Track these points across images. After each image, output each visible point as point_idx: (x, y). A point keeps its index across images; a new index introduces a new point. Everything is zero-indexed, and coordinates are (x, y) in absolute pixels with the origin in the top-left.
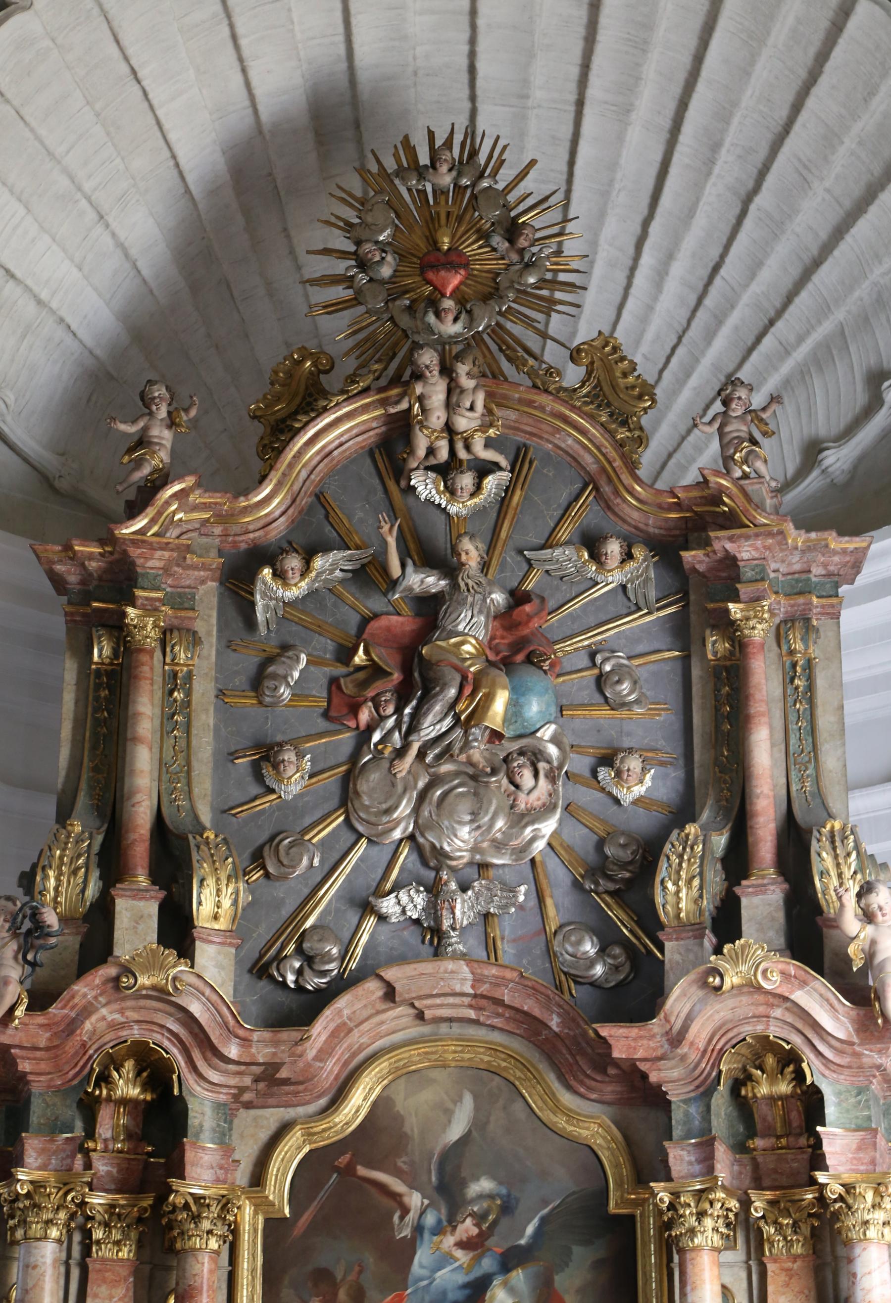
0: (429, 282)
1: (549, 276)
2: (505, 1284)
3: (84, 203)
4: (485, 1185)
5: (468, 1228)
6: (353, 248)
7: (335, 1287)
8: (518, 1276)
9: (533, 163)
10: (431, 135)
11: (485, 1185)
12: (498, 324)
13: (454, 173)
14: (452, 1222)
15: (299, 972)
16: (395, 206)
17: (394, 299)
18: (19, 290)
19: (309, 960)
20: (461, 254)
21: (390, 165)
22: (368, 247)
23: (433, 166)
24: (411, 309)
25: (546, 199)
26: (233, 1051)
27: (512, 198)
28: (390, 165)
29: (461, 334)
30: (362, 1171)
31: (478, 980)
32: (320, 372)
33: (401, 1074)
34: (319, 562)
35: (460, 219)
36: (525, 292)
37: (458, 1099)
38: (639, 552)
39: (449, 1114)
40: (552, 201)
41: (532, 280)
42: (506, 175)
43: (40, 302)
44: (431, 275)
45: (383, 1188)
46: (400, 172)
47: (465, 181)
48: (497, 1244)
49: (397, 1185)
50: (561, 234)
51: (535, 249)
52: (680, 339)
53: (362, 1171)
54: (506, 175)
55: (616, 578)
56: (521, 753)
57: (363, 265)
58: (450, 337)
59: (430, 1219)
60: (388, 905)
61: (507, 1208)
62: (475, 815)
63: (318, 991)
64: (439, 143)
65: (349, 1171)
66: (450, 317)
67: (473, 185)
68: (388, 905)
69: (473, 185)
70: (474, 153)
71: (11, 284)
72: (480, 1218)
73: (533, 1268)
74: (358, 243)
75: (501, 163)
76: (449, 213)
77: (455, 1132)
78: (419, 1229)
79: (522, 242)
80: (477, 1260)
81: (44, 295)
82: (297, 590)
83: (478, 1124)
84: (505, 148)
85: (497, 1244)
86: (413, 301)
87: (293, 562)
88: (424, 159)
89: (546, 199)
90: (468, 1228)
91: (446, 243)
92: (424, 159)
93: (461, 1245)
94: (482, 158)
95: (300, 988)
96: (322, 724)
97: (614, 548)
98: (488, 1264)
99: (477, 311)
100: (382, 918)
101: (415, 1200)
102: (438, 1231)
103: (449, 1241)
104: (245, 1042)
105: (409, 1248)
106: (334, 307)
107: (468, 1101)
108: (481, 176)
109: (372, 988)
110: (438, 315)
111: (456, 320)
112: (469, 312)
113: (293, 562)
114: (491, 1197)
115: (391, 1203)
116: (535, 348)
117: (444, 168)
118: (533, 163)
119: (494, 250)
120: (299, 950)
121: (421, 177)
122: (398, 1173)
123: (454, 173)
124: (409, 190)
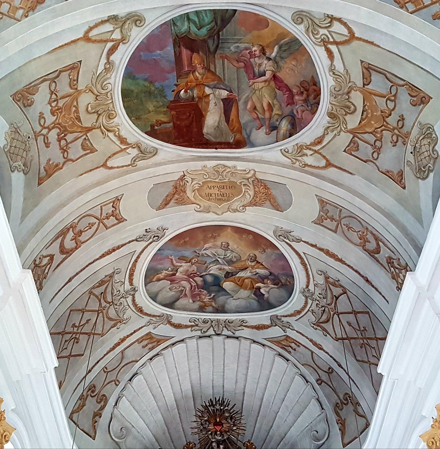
0: (215, 428)
1: (238, 427)
3: (149, 412)
6: (200, 421)
9: (235, 404)
10: (216, 398)
12: (229, 437)
13: (220, 406)
16: (208, 412)
17: (208, 432)
18: (135, 429)
20: (221, 423)
21: (208, 404)
22: (203, 421)
23: (216, 405)
24: (211, 434)
25: (238, 412)
27: (231, 411)
28: (208, 404)
29: (221, 439)
32: (193, 447)
35: (221, 415)
36: (234, 431)
40: (239, 412)
41: (235, 428)
42: (230, 407)
43: (138, 432)
44: (215, 427)
46: (210, 406)
47: (222, 408)
50: (241, 419)
51: (236, 422)
52: (264, 442)
54: (230, 407)
58: (219, 440)
64: (217, 400)
66: (219, 435)
67: (224, 408)
69: (224, 408)
70: (224, 402)
71: (133, 429)
74: (201, 420)
75: (229, 404)
76: (219, 414)
79: (233, 420)
81: (139, 431)
84: (230, 401)
86: (212, 432)
89: (238, 412)
91: (218, 420)
99: (224, 435)
106: (196, 433)
108: (225, 407)
110: (217, 435)
111: (220, 436)
112: (223, 435)
116: (236, 442)
117: (218, 405)
118: (235, 404)
119: (228, 422)
121: (214, 407)
123: (220, 406)
124: (211, 409)
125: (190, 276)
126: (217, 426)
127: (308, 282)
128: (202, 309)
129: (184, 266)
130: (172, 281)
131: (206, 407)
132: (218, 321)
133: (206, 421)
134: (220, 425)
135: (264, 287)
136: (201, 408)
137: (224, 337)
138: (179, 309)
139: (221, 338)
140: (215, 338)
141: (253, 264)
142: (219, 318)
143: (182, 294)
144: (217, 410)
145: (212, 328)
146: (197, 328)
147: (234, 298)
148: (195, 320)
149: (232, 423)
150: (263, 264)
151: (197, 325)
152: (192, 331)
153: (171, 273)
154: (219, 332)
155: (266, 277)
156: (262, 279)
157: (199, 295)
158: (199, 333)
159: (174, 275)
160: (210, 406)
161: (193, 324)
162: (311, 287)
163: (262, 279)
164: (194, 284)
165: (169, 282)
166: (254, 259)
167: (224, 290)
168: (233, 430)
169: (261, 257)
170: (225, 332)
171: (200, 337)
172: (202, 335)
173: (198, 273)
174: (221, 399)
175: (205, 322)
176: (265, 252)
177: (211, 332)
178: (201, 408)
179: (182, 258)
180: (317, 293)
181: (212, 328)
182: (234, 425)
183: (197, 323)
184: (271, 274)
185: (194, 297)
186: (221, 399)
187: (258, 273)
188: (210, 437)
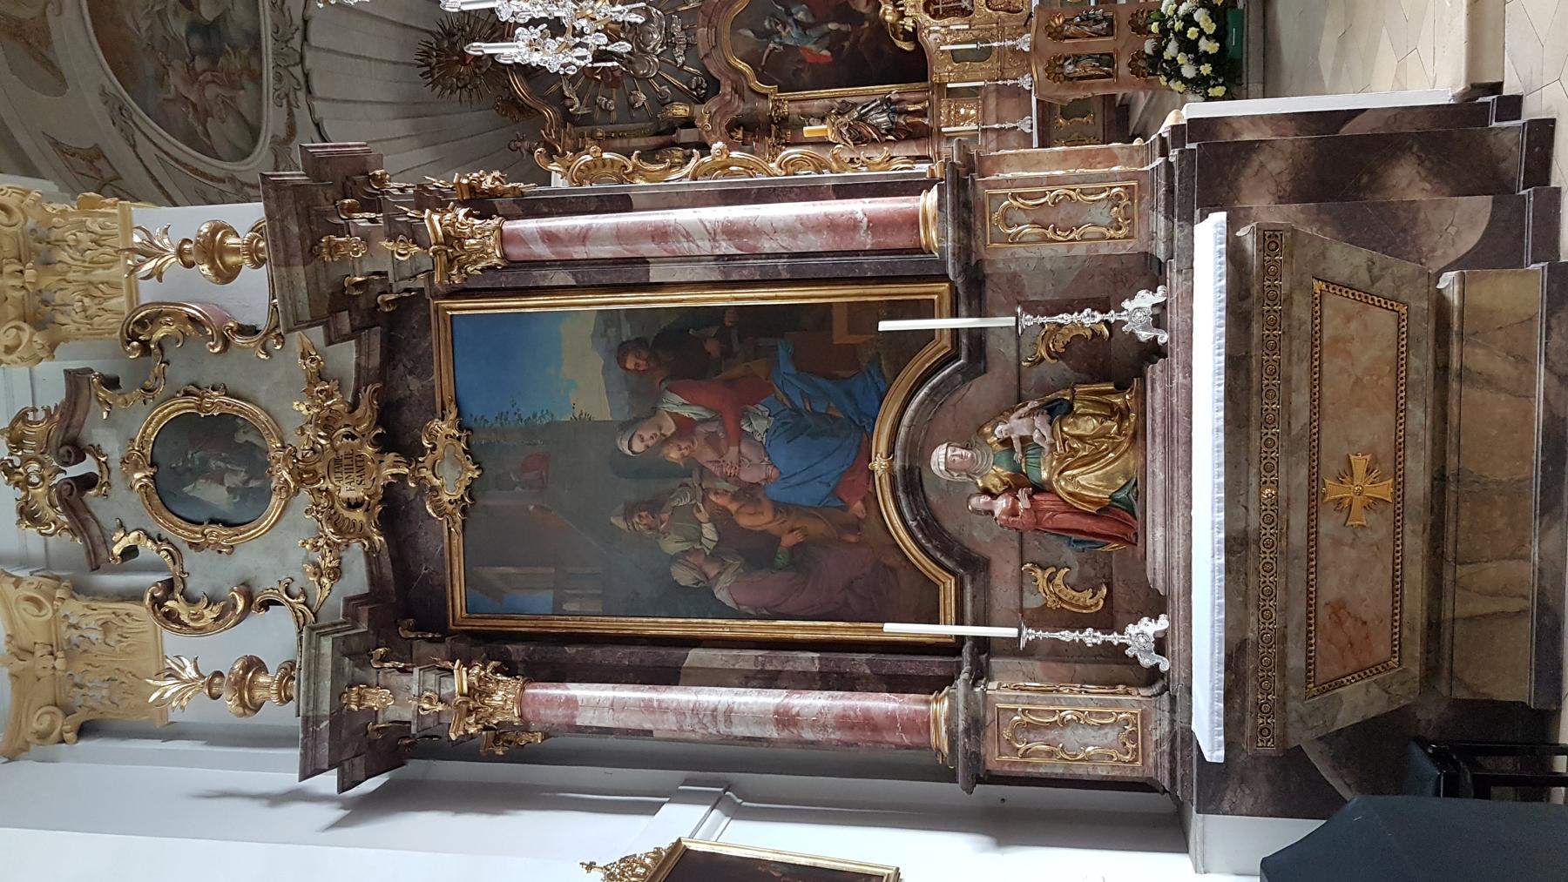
2: (797, 14)
4: (766, 23)
5: (779, 27)
7: (798, 69)
8: (793, 11)
11: (766, 23)
14: (778, 32)
15: (702, 89)
16: (443, 76)
19: (698, 86)
24: (480, 68)
26: (728, 97)
27: (440, 37)
30: (763, 64)
33: (734, 51)
34: (567, 93)
37: (740, 34)
39: (746, 37)
45: (768, 56)
46: (432, 76)
48: (785, 18)
49: (767, 51)
53: (763, 64)
57: (465, 86)
59: (777, 40)
60: (680, 60)
61: (774, 16)
62: (650, 33)
63: (707, 82)
65: (762, 67)
68: (680, 60)
70: (425, 52)
72: (777, 24)
75: (427, 42)
77: (749, 33)
78: (780, 44)
82: (576, 99)
85: (785, 18)
87: (568, 103)
88: (428, 68)
91: (456, 58)
92: (428, 69)
93: (785, 30)
94: (426, 48)
95: (707, 88)
96: (621, 88)
98: (790, 21)
100: (684, 64)
101: (771, 45)
102: (780, 37)
103: (783, 33)
104: (725, 94)
105: (786, 46)
106: (480, 95)
107: (741, 31)
108: (433, 48)
109: (705, 61)
113: (568, 103)
114: (770, 21)
115: (772, 54)
120: (695, 90)
121: (433, 68)
122: (764, 52)
125: (192, 77)
128: (257, 78)
129: (175, 80)
130: (208, 113)
131: (435, 83)
132: (276, 54)
133: (458, 79)
136: (438, 89)
137: (305, 47)
138: (259, 119)
139: (308, 55)
140: (308, 64)
142: (270, 52)
143: (229, 105)
144: (439, 62)
145: (291, 69)
146: (291, 96)
147: (230, 6)
148: (278, 96)
149: (460, 34)
151: (287, 95)
152: (298, 107)
153: (191, 110)
154: (297, 57)
157: (229, 74)
158: (301, 95)
159: (194, 105)
160: (432, 76)
161: (284, 101)
164: (208, 75)
165: (209, 119)
167: (216, 20)
168: (472, 31)
170: (296, 42)
171: (309, 91)
172: (304, 90)
173: (187, 60)
174: (420, 57)
175: (279, 78)
177: (297, 71)
178: (438, 89)
179: (161, 80)
181: (291, 69)
182: (463, 29)
183: (283, 95)
185: (233, 85)
186: (420, 57)
188: (484, 70)
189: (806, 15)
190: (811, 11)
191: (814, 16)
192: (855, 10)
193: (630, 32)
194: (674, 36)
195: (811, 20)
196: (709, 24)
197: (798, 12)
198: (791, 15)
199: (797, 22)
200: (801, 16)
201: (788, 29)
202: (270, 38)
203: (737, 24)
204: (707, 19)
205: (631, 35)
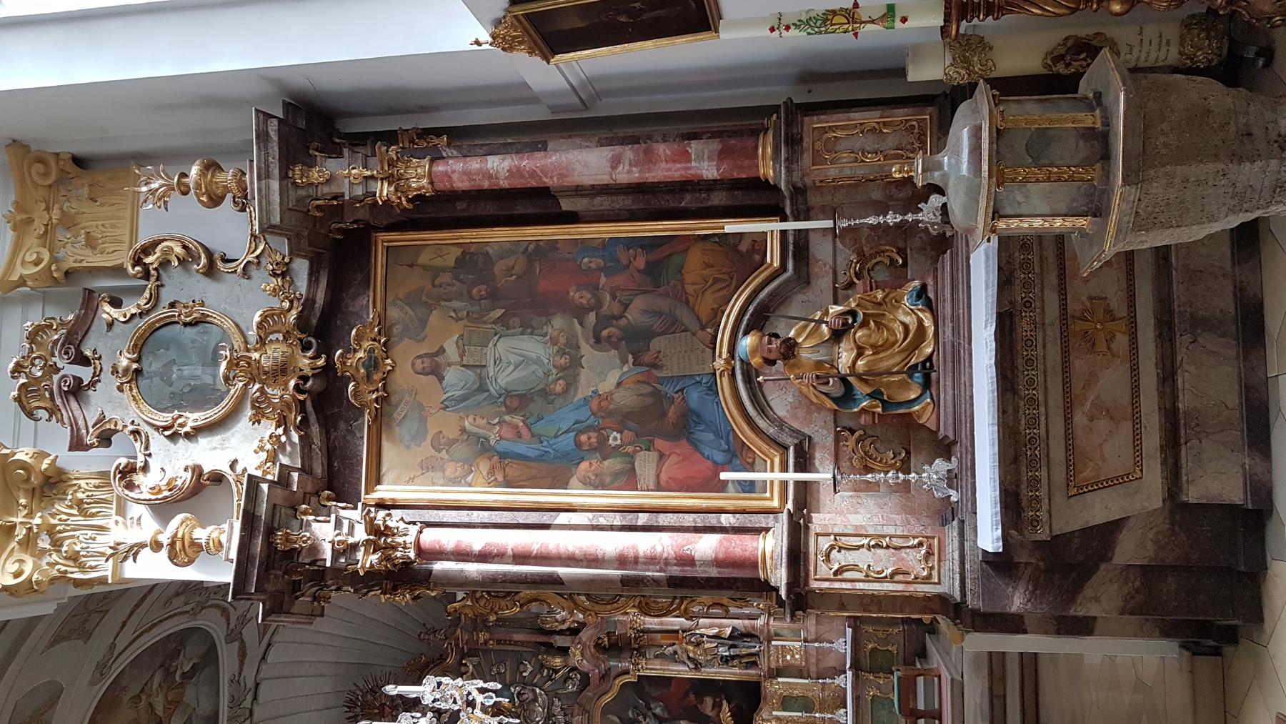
4: (630, 713)
5: (640, 718)
8: (652, 706)
11: (630, 713)
31: (578, 715)
38: (464, 662)
39: (612, 721)
48: (645, 711)
55: (471, 667)
56: (518, 697)
72: (638, 715)
73: (651, 702)
77: (617, 720)
80: (649, 717)
83: (614, 714)
90: (640, 718)
97: (463, 669)
98: (650, 714)
107: (609, 716)
126: (384, 713)
127: (180, 613)
134: (384, 709)
135: (181, 668)
141: (144, 697)
150: (144, 682)
155: (167, 669)
156: (169, 674)
162: (188, 608)
163: (169, 674)
166: (137, 699)
169: (135, 689)
176: (125, 687)
180: (198, 599)
184: (161, 666)
187: (160, 685)
189: (662, 710)
190: (666, 708)
191: (669, 713)
192: (702, 713)
193: (518, 707)
194: (554, 715)
195: (666, 716)
196: (585, 711)
197: (656, 708)
198: (651, 709)
199: (655, 715)
200: (658, 711)
201: (648, 720)
202: (226, 707)
203: (606, 710)
204: (582, 709)
205: (519, 710)
